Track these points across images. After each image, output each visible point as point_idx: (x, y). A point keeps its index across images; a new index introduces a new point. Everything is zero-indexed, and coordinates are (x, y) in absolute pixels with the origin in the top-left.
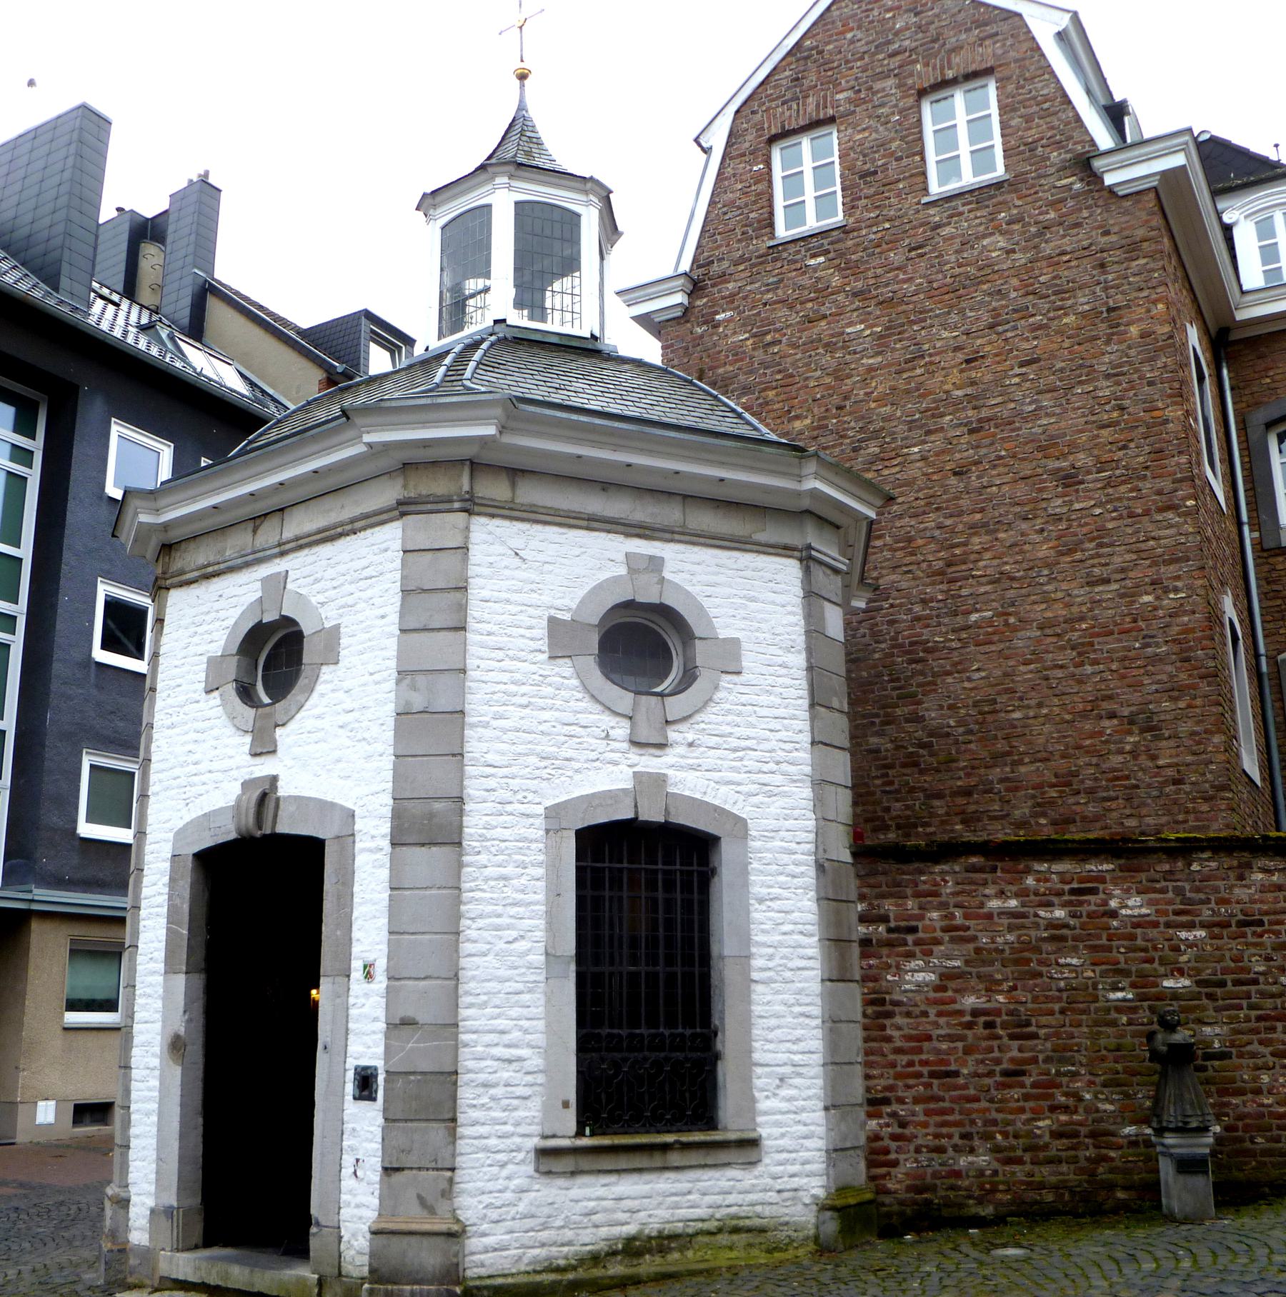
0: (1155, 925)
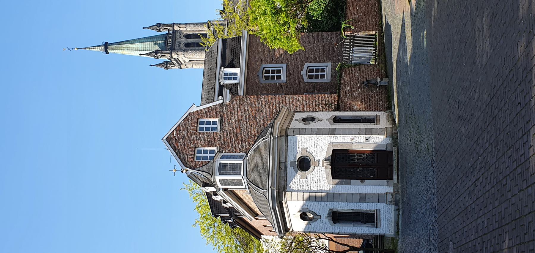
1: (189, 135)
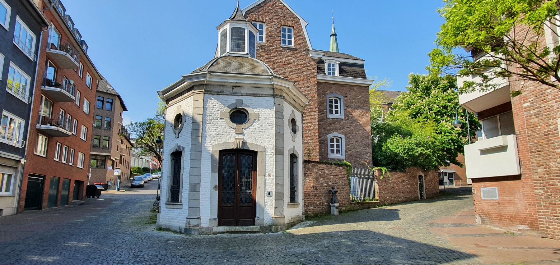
1: (278, 17)
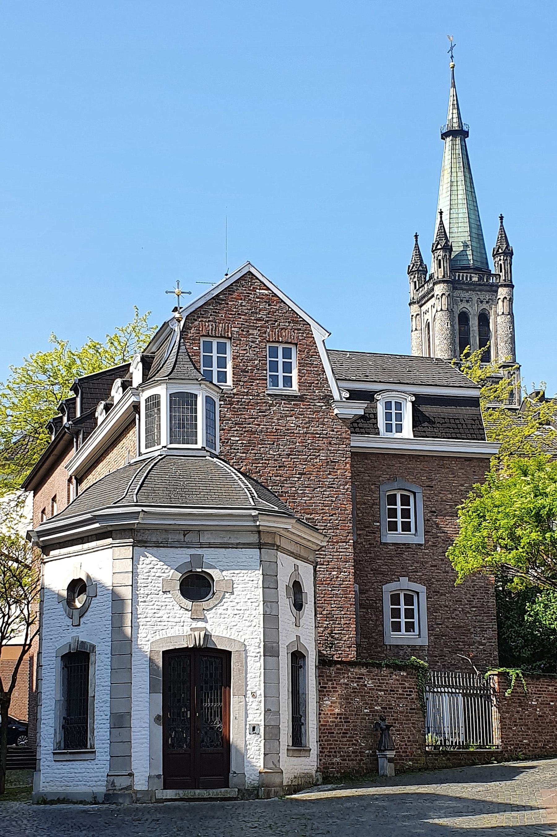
0: (374, 689)
1: (260, 324)
